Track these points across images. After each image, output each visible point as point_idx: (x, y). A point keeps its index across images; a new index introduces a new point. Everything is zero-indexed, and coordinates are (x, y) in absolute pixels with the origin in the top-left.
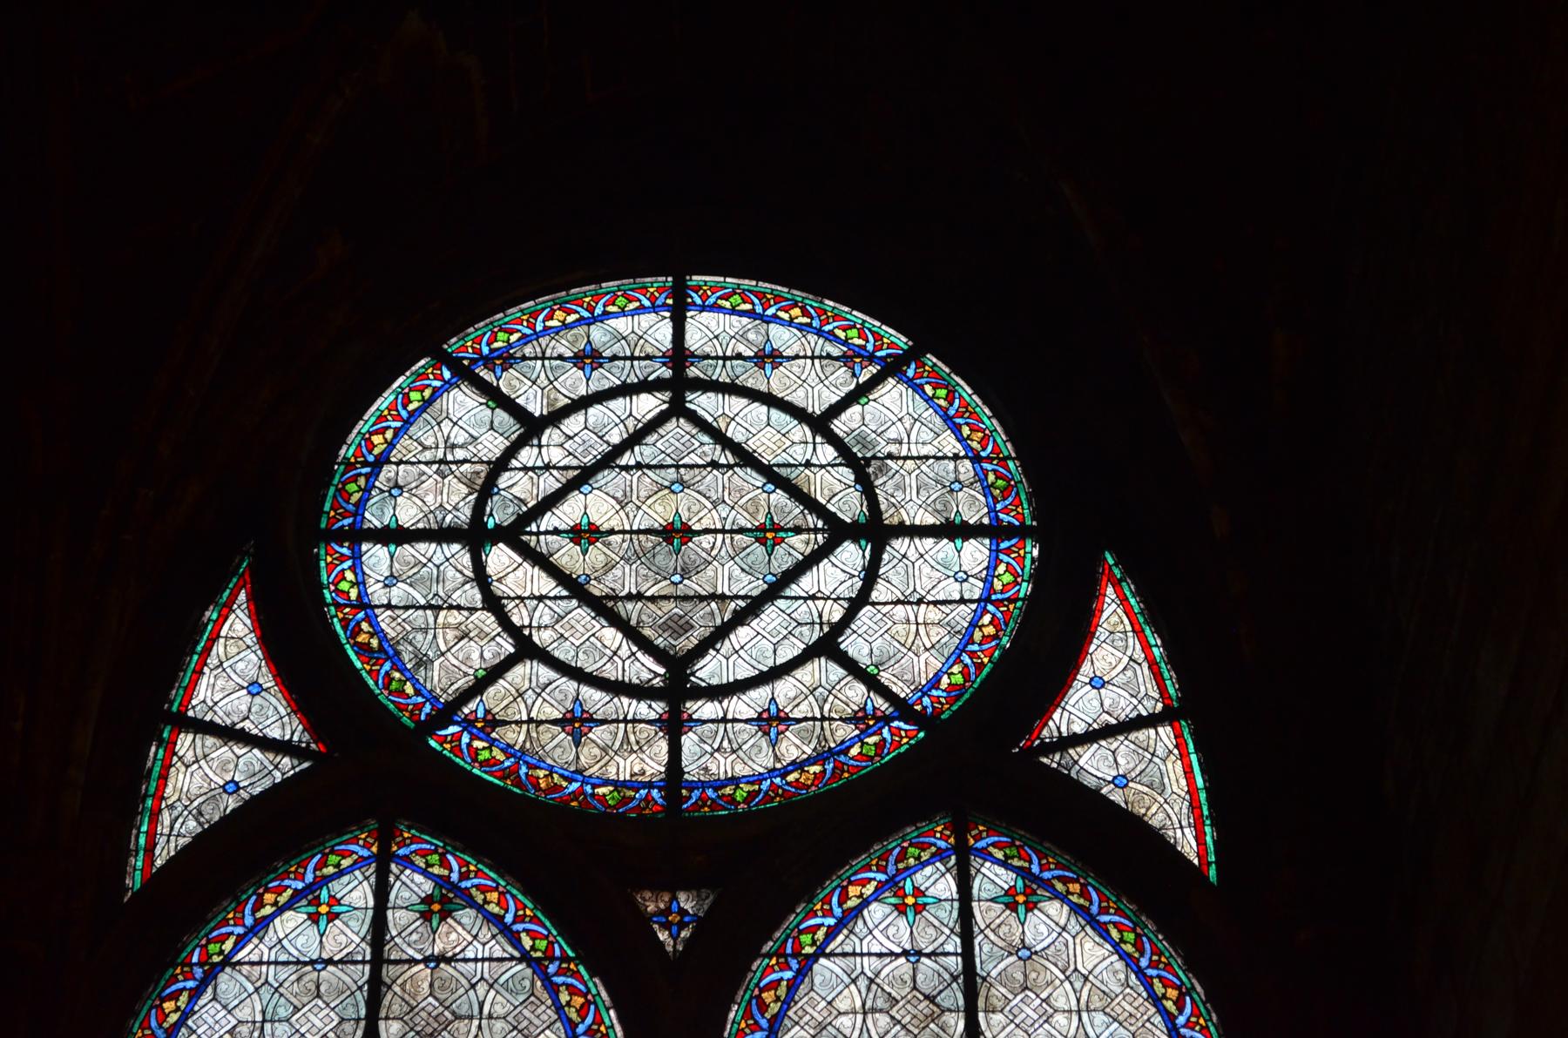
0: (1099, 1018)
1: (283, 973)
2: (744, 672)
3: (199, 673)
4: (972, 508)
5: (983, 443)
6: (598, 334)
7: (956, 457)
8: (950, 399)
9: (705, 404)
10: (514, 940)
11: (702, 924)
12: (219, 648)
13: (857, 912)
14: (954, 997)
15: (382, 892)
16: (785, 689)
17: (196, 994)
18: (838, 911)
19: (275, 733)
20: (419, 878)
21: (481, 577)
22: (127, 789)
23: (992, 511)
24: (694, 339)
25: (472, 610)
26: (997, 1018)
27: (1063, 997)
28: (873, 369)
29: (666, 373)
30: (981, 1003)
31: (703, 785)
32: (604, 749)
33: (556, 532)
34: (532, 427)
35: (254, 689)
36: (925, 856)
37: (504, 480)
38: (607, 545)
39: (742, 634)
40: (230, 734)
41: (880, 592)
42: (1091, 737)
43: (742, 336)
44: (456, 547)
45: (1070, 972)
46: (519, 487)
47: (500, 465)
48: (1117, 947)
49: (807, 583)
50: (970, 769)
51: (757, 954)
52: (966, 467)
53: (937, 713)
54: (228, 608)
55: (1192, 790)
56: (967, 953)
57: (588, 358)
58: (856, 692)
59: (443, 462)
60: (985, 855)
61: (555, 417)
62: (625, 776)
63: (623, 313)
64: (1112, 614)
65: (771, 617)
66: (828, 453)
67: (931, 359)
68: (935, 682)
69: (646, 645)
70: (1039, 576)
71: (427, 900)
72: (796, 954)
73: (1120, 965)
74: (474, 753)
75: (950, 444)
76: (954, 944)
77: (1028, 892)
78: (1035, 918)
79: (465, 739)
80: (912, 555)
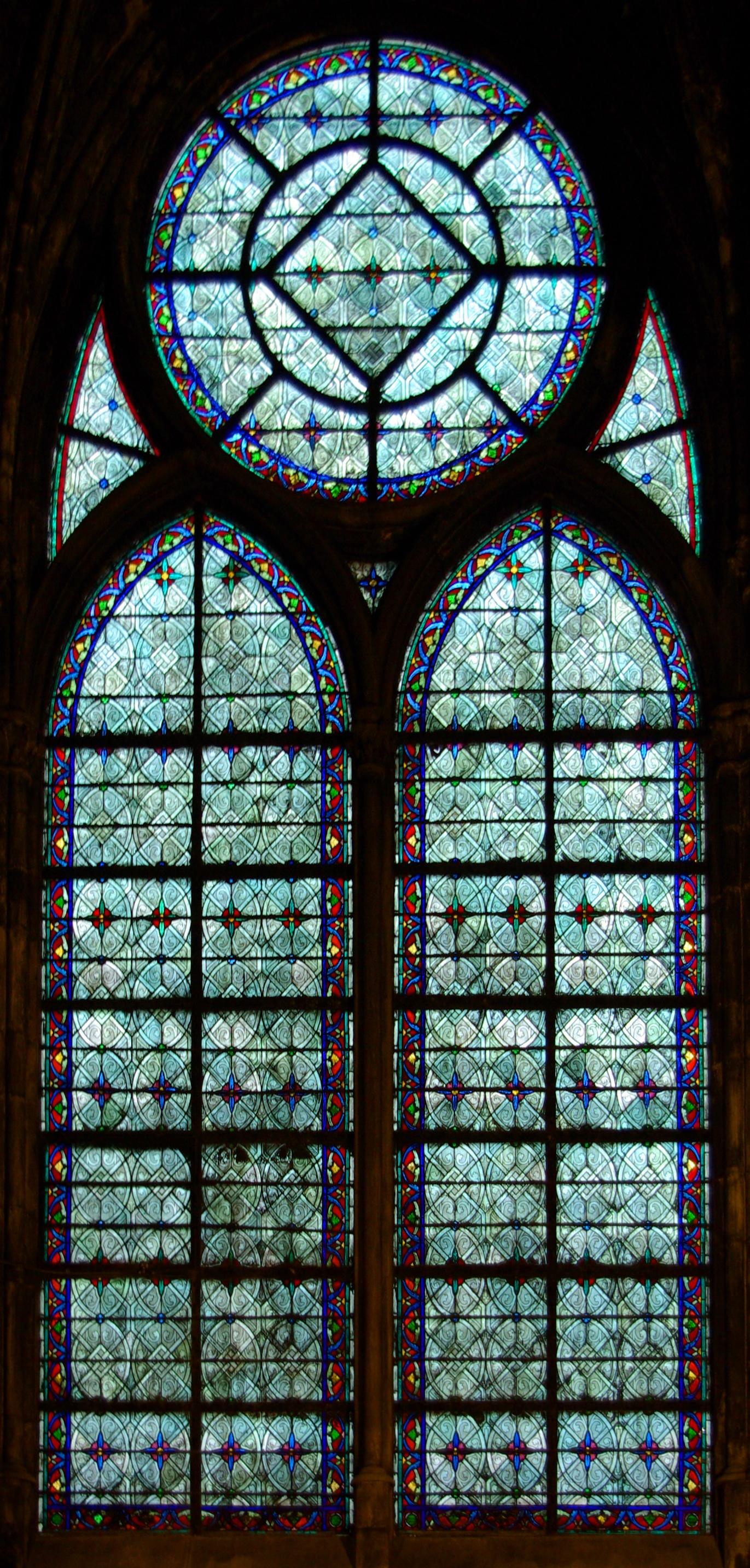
0: (623, 657)
1: (146, 623)
2: (417, 390)
3: (77, 392)
4: (565, 256)
5: (574, 192)
6: (319, 95)
7: (555, 206)
8: (554, 152)
9: (391, 158)
10: (279, 601)
11: (389, 585)
12: (88, 373)
13: (480, 580)
14: (538, 642)
16: (442, 403)
18: (471, 578)
19: (127, 441)
20: (220, 553)
21: (249, 313)
22: (42, 484)
23: (577, 255)
24: (384, 101)
26: (563, 657)
27: (603, 643)
28: (503, 126)
29: (364, 130)
30: (554, 647)
31: (389, 481)
32: (330, 453)
33: (296, 273)
34: (278, 180)
35: (113, 405)
36: (525, 536)
37: (262, 229)
38: (329, 283)
39: (415, 360)
40: (102, 442)
41: (505, 323)
43: (415, 96)
44: (233, 286)
45: (608, 623)
46: (273, 233)
47: (258, 214)
49: (456, 317)
51: (422, 610)
53: (536, 423)
55: (690, 486)
56: (547, 610)
57: (314, 118)
58: (485, 407)
59: (221, 212)
60: (562, 537)
61: (294, 170)
62: (342, 475)
63: (336, 76)
64: (650, 343)
65: (434, 342)
66: (470, 203)
71: (226, 569)
72: (446, 609)
73: (637, 619)
74: (250, 456)
75: (552, 195)
76: (539, 603)
77: (586, 564)
78: (589, 583)
79: (244, 445)
80: (524, 292)
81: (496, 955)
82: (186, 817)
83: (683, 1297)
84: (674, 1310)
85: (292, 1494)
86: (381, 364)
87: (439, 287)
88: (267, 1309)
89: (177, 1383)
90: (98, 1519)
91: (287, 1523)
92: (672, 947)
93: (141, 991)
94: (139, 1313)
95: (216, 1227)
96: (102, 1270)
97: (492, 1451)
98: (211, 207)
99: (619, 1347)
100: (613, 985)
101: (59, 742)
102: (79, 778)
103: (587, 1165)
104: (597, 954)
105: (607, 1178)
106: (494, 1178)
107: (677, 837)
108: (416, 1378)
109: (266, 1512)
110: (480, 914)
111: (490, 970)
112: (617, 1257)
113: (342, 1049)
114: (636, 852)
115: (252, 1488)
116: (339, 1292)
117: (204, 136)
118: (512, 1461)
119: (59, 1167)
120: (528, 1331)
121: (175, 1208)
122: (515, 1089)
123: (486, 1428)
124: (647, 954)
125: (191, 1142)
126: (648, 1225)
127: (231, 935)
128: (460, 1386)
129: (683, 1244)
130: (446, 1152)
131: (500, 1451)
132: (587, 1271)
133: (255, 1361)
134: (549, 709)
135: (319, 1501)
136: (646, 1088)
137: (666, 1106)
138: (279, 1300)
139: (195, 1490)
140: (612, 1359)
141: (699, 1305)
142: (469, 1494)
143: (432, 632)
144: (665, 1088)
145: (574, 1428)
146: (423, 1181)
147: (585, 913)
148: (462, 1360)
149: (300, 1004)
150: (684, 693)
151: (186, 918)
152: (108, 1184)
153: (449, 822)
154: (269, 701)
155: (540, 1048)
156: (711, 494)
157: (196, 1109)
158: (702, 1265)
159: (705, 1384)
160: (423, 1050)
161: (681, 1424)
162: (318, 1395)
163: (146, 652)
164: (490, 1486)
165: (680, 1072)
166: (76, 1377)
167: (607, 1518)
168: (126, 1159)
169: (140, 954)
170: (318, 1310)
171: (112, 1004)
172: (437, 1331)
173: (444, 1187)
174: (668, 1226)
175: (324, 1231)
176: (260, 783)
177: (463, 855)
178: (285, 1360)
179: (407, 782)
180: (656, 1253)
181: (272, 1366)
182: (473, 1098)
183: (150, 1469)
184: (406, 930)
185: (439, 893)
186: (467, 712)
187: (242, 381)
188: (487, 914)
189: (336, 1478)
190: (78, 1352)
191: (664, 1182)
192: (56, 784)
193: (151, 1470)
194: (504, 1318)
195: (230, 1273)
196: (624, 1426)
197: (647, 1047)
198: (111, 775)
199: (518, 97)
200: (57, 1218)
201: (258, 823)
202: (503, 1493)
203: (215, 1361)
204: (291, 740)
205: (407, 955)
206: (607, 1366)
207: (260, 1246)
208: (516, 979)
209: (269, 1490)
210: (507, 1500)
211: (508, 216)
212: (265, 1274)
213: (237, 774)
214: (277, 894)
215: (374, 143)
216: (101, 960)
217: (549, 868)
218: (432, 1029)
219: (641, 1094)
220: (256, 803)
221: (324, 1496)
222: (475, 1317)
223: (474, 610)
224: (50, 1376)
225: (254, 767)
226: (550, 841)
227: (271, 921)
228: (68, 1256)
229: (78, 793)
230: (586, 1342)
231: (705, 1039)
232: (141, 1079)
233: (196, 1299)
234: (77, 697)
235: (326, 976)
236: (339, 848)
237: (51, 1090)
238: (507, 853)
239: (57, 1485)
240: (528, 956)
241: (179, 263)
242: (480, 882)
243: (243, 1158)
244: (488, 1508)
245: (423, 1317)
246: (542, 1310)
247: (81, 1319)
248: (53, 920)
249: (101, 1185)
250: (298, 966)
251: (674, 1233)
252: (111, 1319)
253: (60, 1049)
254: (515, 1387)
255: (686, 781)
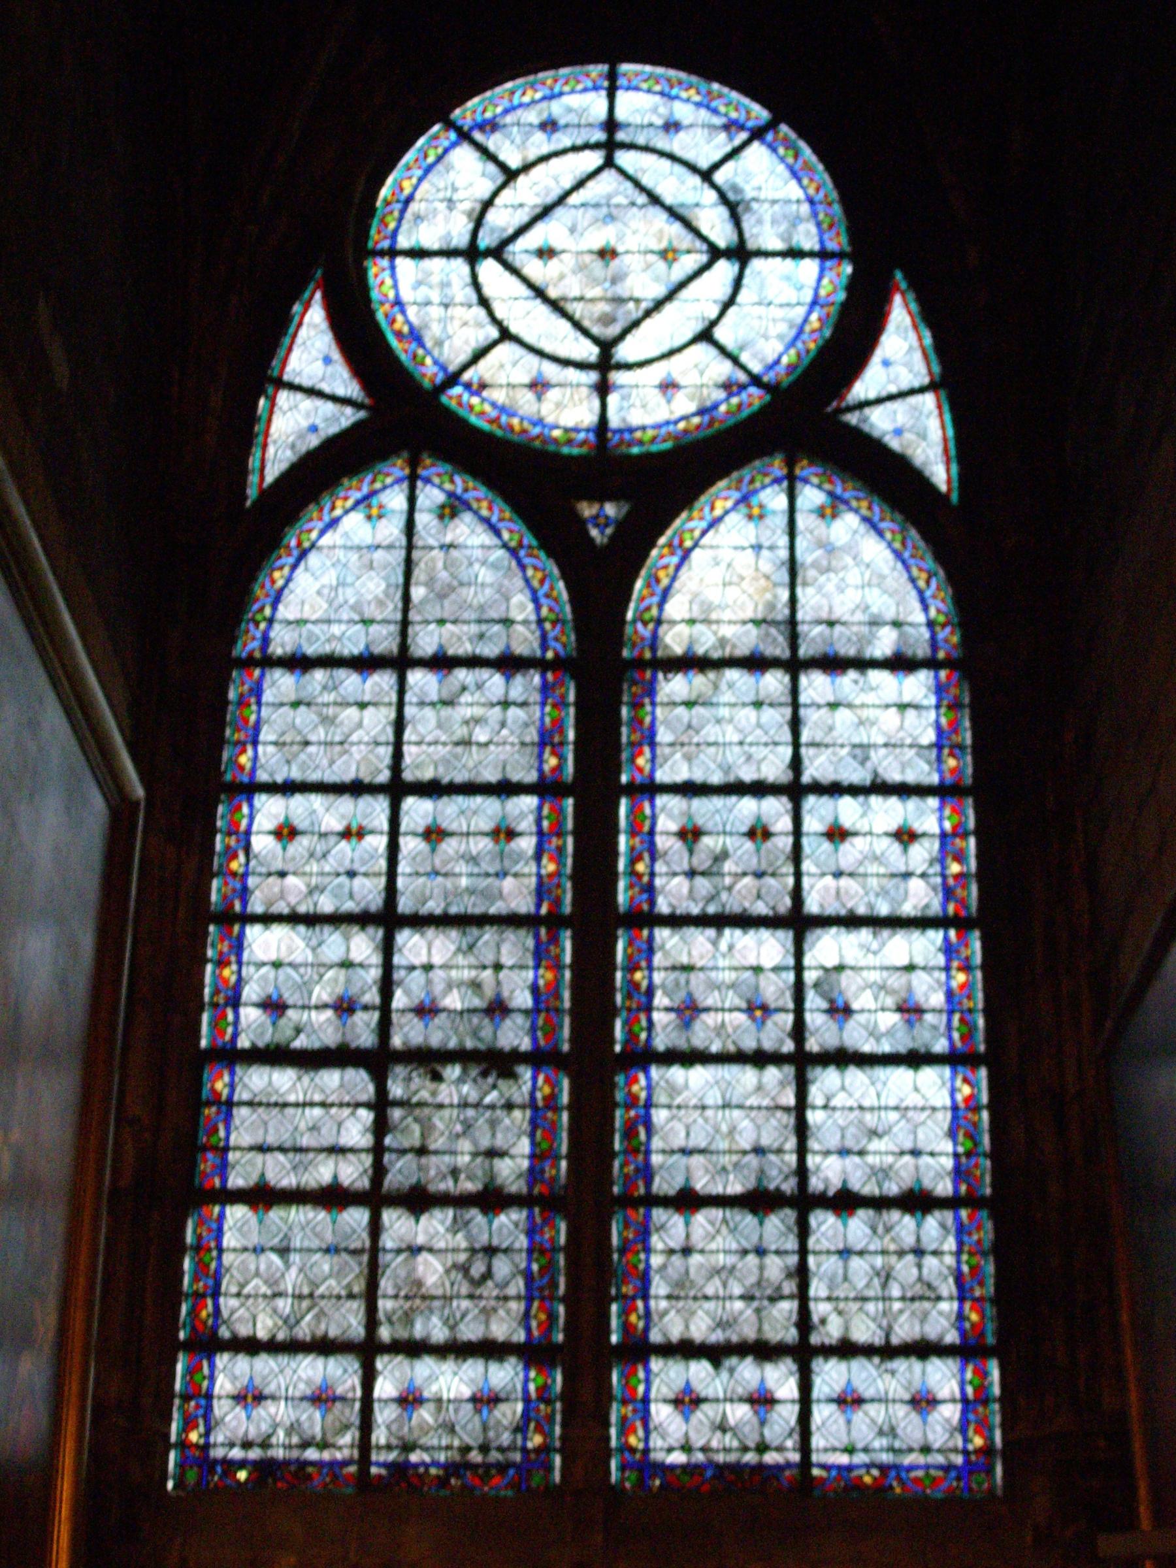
0: (876, 591)
3: (290, 349)
4: (808, 239)
6: (556, 108)
7: (798, 201)
8: (796, 156)
9: (623, 158)
10: (497, 533)
15: (412, 500)
17: (294, 567)
19: (341, 392)
22: (245, 431)
24: (621, 114)
25: (470, 306)
26: (810, 591)
27: (854, 576)
30: (799, 580)
31: (620, 431)
34: (510, 175)
35: (327, 360)
40: (313, 392)
42: (879, 401)
43: (655, 110)
46: (501, 219)
47: (488, 204)
48: (890, 545)
50: (797, 423)
52: (805, 208)
54: (307, 306)
55: (945, 439)
57: (549, 126)
60: (806, 481)
61: (527, 168)
62: (570, 424)
63: (573, 92)
67: (784, 129)
68: (777, 362)
69: (586, 333)
70: (852, 286)
71: (443, 507)
74: (471, 408)
76: (784, 541)
77: (834, 507)
81: (736, 875)
82: (390, 734)
83: (961, 1231)
84: (950, 1244)
85: (484, 1448)
86: (613, 330)
87: (676, 266)
88: (461, 1240)
89: (349, 1321)
90: (242, 1475)
91: (477, 1482)
92: (937, 868)
93: (326, 905)
94: (306, 1244)
95: (403, 1152)
96: (262, 1197)
97: (732, 1400)
98: (441, 195)
99: (884, 1286)
100: (871, 906)
101: (249, 663)
102: (268, 696)
103: (843, 1088)
104: (851, 875)
105: (866, 1103)
106: (734, 1101)
107: (939, 759)
108: (639, 1318)
109: (451, 1469)
110: (718, 834)
111: (730, 889)
112: (880, 1187)
113: (557, 966)
114: (894, 776)
115: (435, 1442)
116: (548, 1222)
117: (436, 137)
118: (756, 1412)
119: (219, 1086)
120: (775, 1267)
121: (356, 1130)
122: (758, 1009)
123: (725, 1375)
124: (907, 875)
125: (378, 1060)
126: (915, 1153)
127: (433, 850)
128: (693, 1328)
129: (958, 1173)
130: (677, 1073)
131: (741, 1400)
132: (845, 1202)
133: (444, 1297)
134: (794, 639)
135: (517, 1457)
136: (910, 1010)
137: (935, 1028)
138: (475, 1231)
139: (365, 1444)
140: (876, 1299)
141: (979, 1242)
142: (705, 1449)
143: (666, 567)
144: (934, 1010)
145: (830, 1376)
146: (649, 1105)
147: (837, 834)
148: (695, 1298)
149: (512, 921)
150: (944, 626)
151: (382, 833)
152: (276, 1104)
153: (682, 745)
154: (484, 627)
155: (786, 968)
156: (967, 445)
157: (385, 1027)
158: (983, 1198)
159: (990, 1328)
160: (650, 968)
161: (963, 1371)
162: (520, 1336)
163: (349, 580)
164: (729, 1440)
165: (950, 994)
166: (225, 1313)
167: (875, 1479)
168: (299, 1078)
169: (327, 869)
170: (522, 1241)
171: (293, 919)
172: (664, 1267)
173: (675, 1111)
174: (940, 1154)
175: (533, 1156)
176: (472, 705)
177: (698, 776)
178: (480, 1297)
179: (637, 705)
180: (927, 1183)
181: (465, 1304)
182: (710, 1019)
183: (310, 1418)
184: (633, 849)
185: (669, 813)
186: (705, 642)
187: (467, 342)
188: (725, 833)
189: (539, 1429)
190: (228, 1285)
191: (934, 1109)
192: (243, 703)
193: (314, 1421)
194: (745, 1252)
195: (418, 1201)
196: (893, 1373)
197: (911, 968)
198: (303, 695)
199: (760, 113)
200: (214, 1140)
201: (466, 743)
202: (745, 1449)
203: (396, 1297)
204: (508, 664)
205: (633, 873)
206: (871, 1307)
207: (455, 1172)
208: (759, 897)
209: (456, 1443)
210: (750, 1457)
211: (748, 209)
212: (460, 1201)
213: (445, 695)
214: (487, 810)
215: (610, 147)
216: (282, 874)
217: (795, 790)
218: (662, 947)
219: (907, 1016)
220: (467, 722)
221: (524, 1450)
222: (712, 1252)
223: (711, 547)
224: (194, 1312)
225: (464, 689)
226: (796, 764)
227: (479, 838)
228: (224, 1180)
229: (265, 712)
230: (846, 1278)
231: (978, 959)
232: (322, 993)
233: (375, 1228)
234: (271, 621)
235: (541, 892)
236: (558, 769)
237: (215, 1005)
238: (748, 775)
239: (194, 1437)
240: (773, 875)
241: (403, 242)
242: (717, 802)
243: (437, 1077)
244: (727, 1467)
245: (648, 1250)
246: (792, 1244)
247: (235, 1250)
248: (229, 834)
249: (268, 1105)
250: (508, 883)
251: (949, 1163)
252: (272, 1249)
253: (228, 963)
254: (760, 1330)
255: (950, 707)
